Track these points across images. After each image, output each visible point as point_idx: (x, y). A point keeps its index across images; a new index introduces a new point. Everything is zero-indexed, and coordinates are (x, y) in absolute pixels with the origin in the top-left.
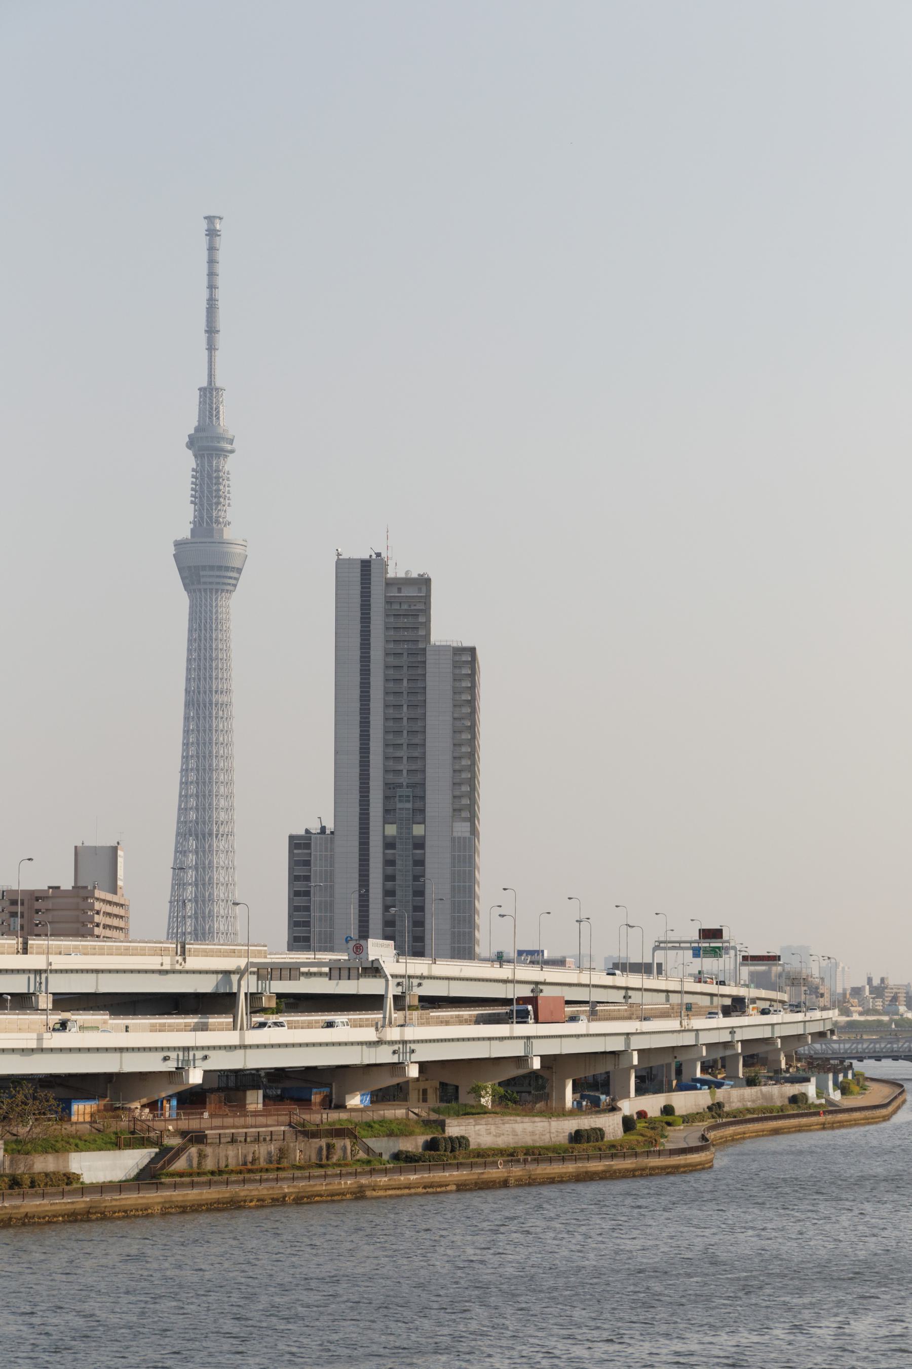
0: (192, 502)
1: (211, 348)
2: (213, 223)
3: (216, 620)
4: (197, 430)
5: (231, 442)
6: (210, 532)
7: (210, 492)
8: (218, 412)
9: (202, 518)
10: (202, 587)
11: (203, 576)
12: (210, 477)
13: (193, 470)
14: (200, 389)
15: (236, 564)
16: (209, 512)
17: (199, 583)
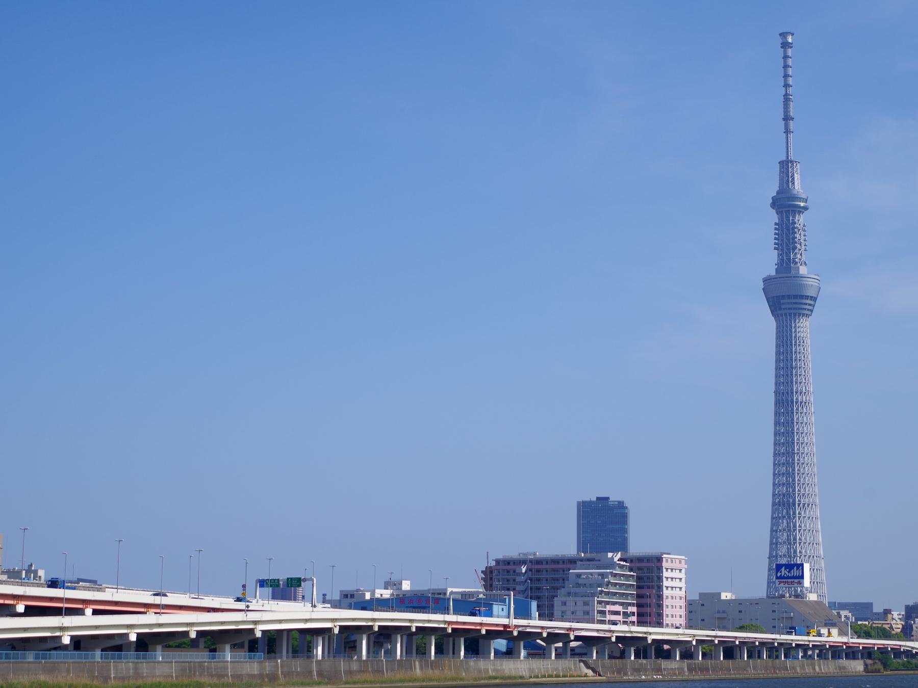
0: (775, 249)
1: (787, 131)
2: (786, 38)
3: (795, 337)
4: (778, 193)
5: (806, 201)
6: (789, 269)
7: (788, 240)
8: (793, 179)
9: (782, 260)
10: (783, 312)
11: (783, 304)
12: (788, 229)
13: (776, 224)
14: (779, 163)
15: (812, 293)
16: (788, 255)
17: (780, 309)
